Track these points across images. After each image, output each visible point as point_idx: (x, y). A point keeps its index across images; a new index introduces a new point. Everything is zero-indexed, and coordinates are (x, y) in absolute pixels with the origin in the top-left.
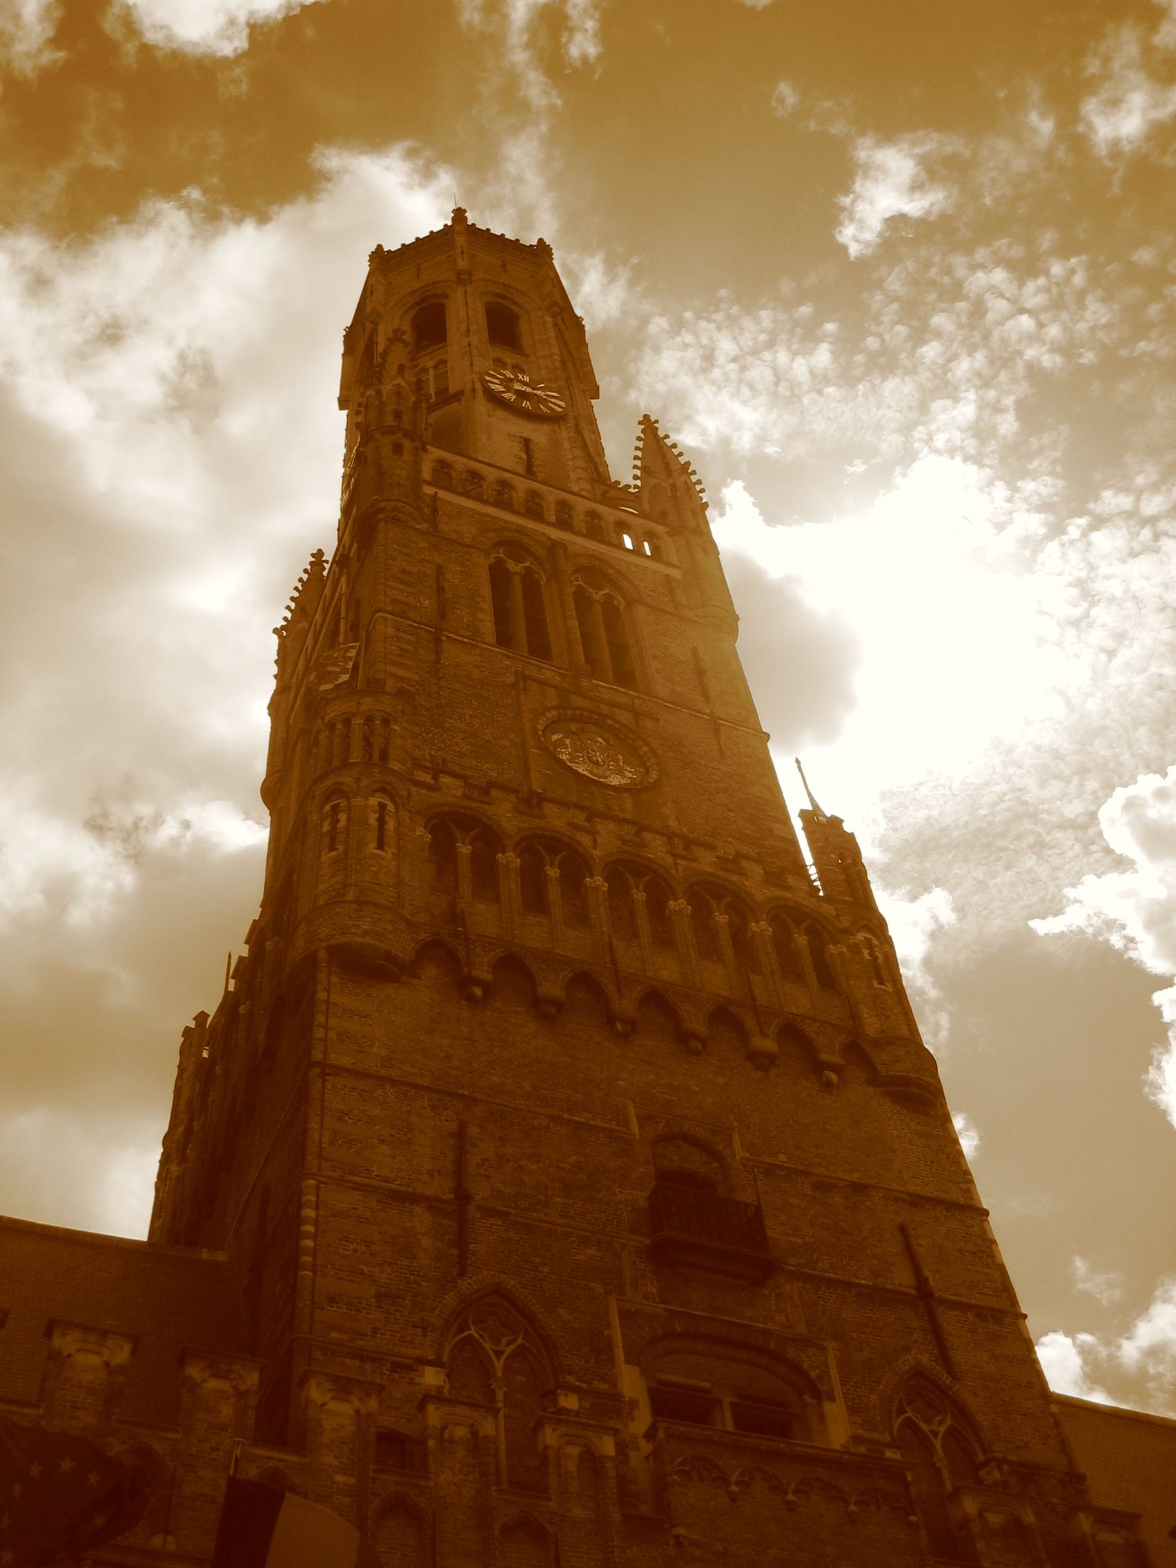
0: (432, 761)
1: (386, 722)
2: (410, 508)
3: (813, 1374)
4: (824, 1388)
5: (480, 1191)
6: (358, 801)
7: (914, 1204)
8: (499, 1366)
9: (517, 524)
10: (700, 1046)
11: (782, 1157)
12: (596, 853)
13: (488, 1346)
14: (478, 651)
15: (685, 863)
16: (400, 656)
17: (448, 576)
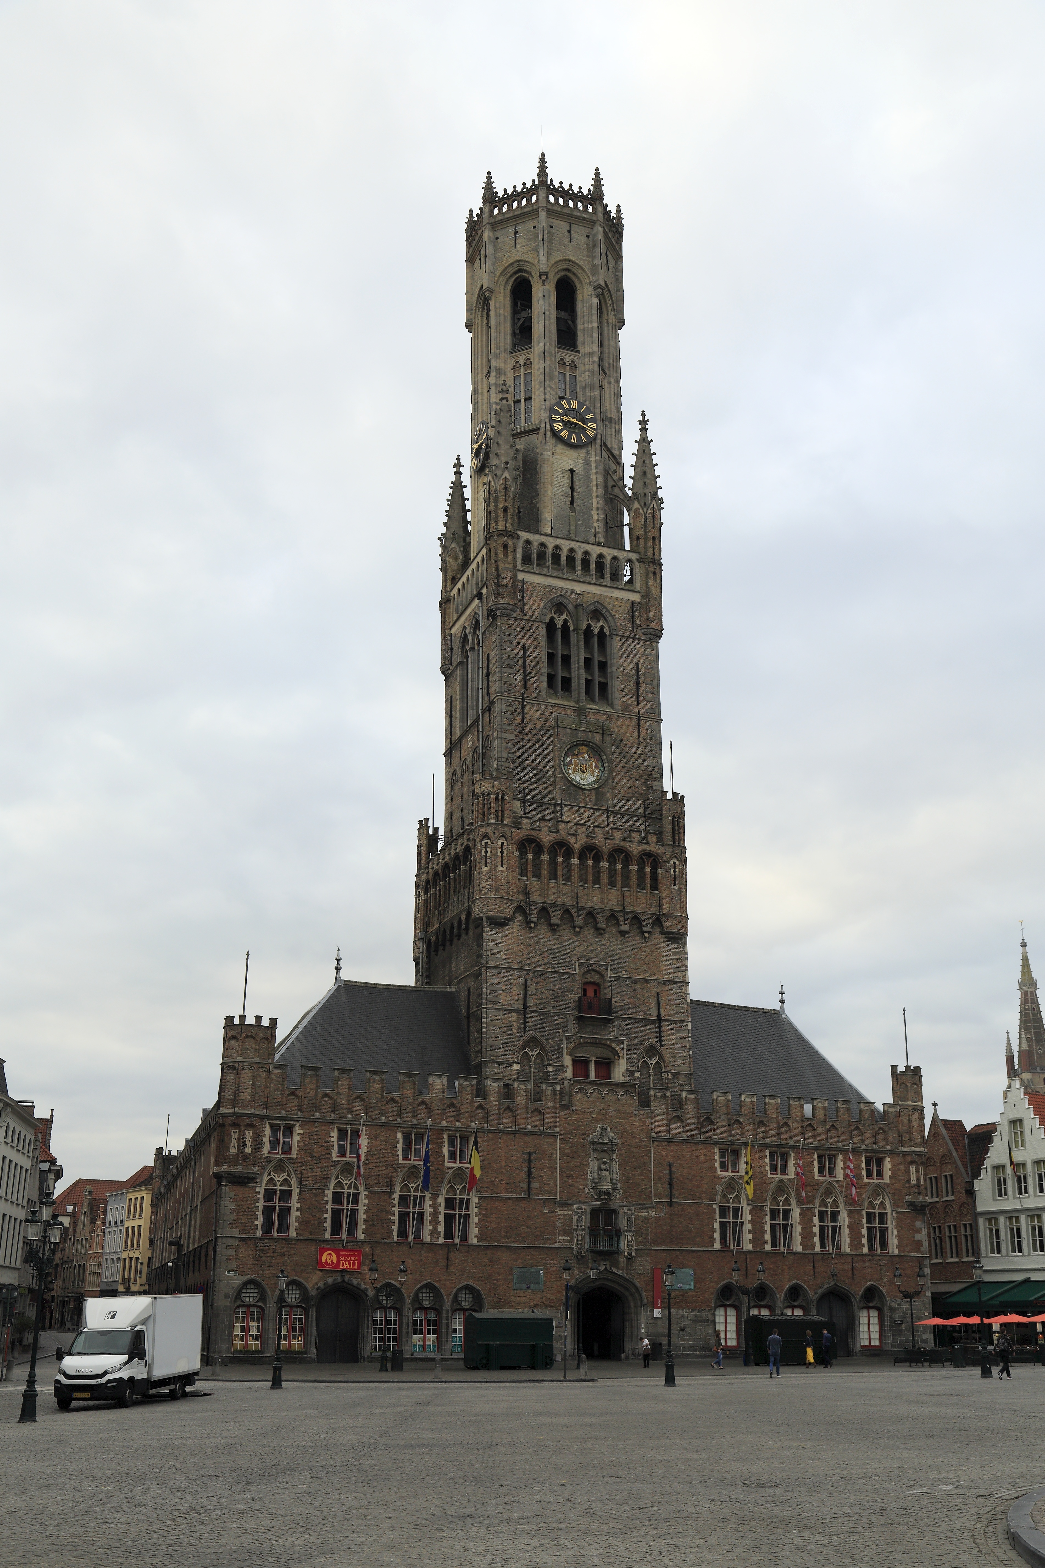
0: (520, 791)
1: (503, 795)
2: (511, 607)
4: (621, 1055)
5: (530, 1004)
6: (494, 845)
7: (664, 984)
8: (533, 1059)
9: (562, 588)
11: (624, 972)
12: (575, 846)
13: (530, 1053)
14: (539, 708)
17: (528, 652)
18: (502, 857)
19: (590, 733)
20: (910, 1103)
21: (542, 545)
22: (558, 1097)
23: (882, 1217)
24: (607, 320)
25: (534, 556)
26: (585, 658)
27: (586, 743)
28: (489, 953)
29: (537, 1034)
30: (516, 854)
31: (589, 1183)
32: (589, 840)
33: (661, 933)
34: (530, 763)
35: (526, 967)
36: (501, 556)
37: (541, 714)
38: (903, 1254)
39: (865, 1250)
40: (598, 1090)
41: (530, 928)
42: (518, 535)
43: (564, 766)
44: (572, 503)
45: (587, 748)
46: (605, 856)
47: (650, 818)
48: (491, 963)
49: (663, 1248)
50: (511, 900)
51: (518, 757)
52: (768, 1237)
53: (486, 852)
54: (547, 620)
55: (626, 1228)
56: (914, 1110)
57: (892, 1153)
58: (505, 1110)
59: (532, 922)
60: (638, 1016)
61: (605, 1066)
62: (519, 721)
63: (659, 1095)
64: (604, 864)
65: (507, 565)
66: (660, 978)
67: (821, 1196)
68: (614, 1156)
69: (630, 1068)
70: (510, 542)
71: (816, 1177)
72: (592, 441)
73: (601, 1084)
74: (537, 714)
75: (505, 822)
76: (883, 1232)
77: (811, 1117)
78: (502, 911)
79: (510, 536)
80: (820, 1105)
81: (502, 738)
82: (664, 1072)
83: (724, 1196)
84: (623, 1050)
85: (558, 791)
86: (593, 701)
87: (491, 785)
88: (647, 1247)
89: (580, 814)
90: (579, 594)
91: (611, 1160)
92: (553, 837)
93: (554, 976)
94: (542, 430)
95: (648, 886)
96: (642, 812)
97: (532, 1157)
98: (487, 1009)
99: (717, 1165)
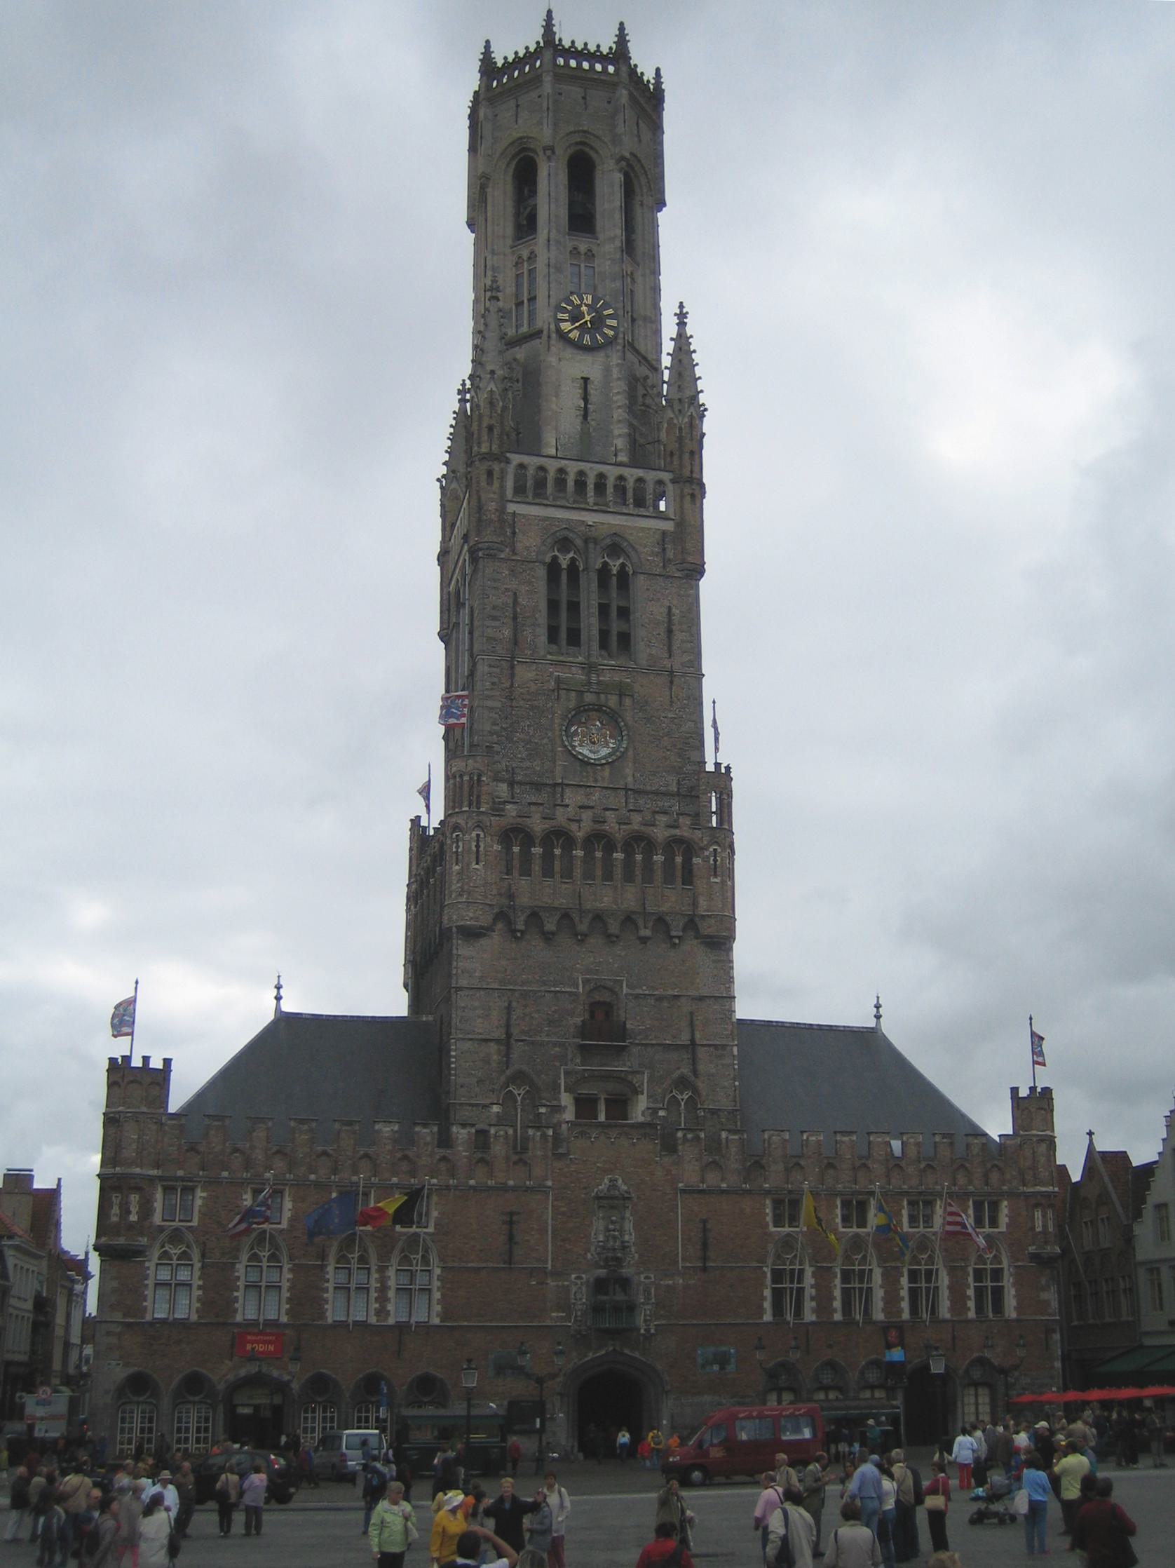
0: (507, 771)
1: (479, 776)
3: (637, 1085)
4: (639, 1089)
5: (515, 1031)
6: (467, 837)
8: (519, 1099)
9: (567, 520)
10: (615, 939)
15: (623, 827)
16: (492, 689)
17: (520, 600)
18: (478, 852)
19: (602, 696)
20: (1034, 1132)
21: (542, 468)
22: (550, 1145)
23: (997, 1274)
24: (642, 202)
25: (530, 483)
26: (600, 604)
27: (599, 708)
28: (459, 971)
29: (524, 1067)
30: (497, 847)
31: (593, 1248)
32: (597, 826)
33: (696, 938)
34: (522, 736)
35: (511, 987)
36: (483, 484)
37: (537, 675)
38: (1023, 1317)
39: (972, 1314)
40: (605, 1133)
41: (517, 938)
42: (507, 458)
43: (567, 737)
44: (585, 416)
45: (598, 714)
46: (619, 846)
47: (685, 796)
48: (463, 982)
49: (695, 1322)
50: (490, 905)
51: (505, 729)
52: (837, 1304)
53: (457, 847)
54: (548, 560)
55: (642, 1300)
56: (1041, 1140)
57: (1010, 1195)
58: (478, 1162)
59: (519, 931)
60: (664, 1042)
61: (619, 1106)
62: (508, 685)
63: (690, 1136)
64: (619, 856)
65: (492, 496)
66: (693, 993)
67: (913, 1251)
68: (628, 1214)
69: (651, 1105)
70: (496, 467)
71: (906, 1227)
72: (610, 342)
73: (609, 1126)
74: (531, 675)
75: (481, 809)
76: (998, 1293)
77: (900, 1155)
78: (477, 919)
79: (497, 459)
80: (912, 1140)
81: (483, 707)
82: (700, 1109)
83: (778, 1257)
84: (643, 1084)
85: (558, 769)
86: (610, 656)
87: (464, 764)
88: (672, 1322)
89: (588, 795)
90: (590, 526)
91: (623, 1218)
92: (547, 825)
93: (549, 996)
94: (545, 333)
95: (679, 880)
96: (676, 790)
97: (514, 1218)
98: (457, 1040)
99: (769, 1219)
